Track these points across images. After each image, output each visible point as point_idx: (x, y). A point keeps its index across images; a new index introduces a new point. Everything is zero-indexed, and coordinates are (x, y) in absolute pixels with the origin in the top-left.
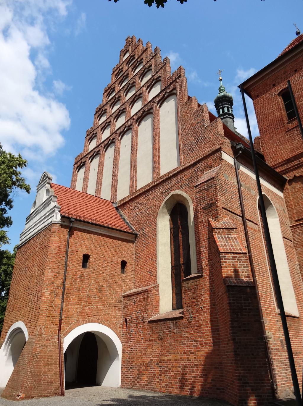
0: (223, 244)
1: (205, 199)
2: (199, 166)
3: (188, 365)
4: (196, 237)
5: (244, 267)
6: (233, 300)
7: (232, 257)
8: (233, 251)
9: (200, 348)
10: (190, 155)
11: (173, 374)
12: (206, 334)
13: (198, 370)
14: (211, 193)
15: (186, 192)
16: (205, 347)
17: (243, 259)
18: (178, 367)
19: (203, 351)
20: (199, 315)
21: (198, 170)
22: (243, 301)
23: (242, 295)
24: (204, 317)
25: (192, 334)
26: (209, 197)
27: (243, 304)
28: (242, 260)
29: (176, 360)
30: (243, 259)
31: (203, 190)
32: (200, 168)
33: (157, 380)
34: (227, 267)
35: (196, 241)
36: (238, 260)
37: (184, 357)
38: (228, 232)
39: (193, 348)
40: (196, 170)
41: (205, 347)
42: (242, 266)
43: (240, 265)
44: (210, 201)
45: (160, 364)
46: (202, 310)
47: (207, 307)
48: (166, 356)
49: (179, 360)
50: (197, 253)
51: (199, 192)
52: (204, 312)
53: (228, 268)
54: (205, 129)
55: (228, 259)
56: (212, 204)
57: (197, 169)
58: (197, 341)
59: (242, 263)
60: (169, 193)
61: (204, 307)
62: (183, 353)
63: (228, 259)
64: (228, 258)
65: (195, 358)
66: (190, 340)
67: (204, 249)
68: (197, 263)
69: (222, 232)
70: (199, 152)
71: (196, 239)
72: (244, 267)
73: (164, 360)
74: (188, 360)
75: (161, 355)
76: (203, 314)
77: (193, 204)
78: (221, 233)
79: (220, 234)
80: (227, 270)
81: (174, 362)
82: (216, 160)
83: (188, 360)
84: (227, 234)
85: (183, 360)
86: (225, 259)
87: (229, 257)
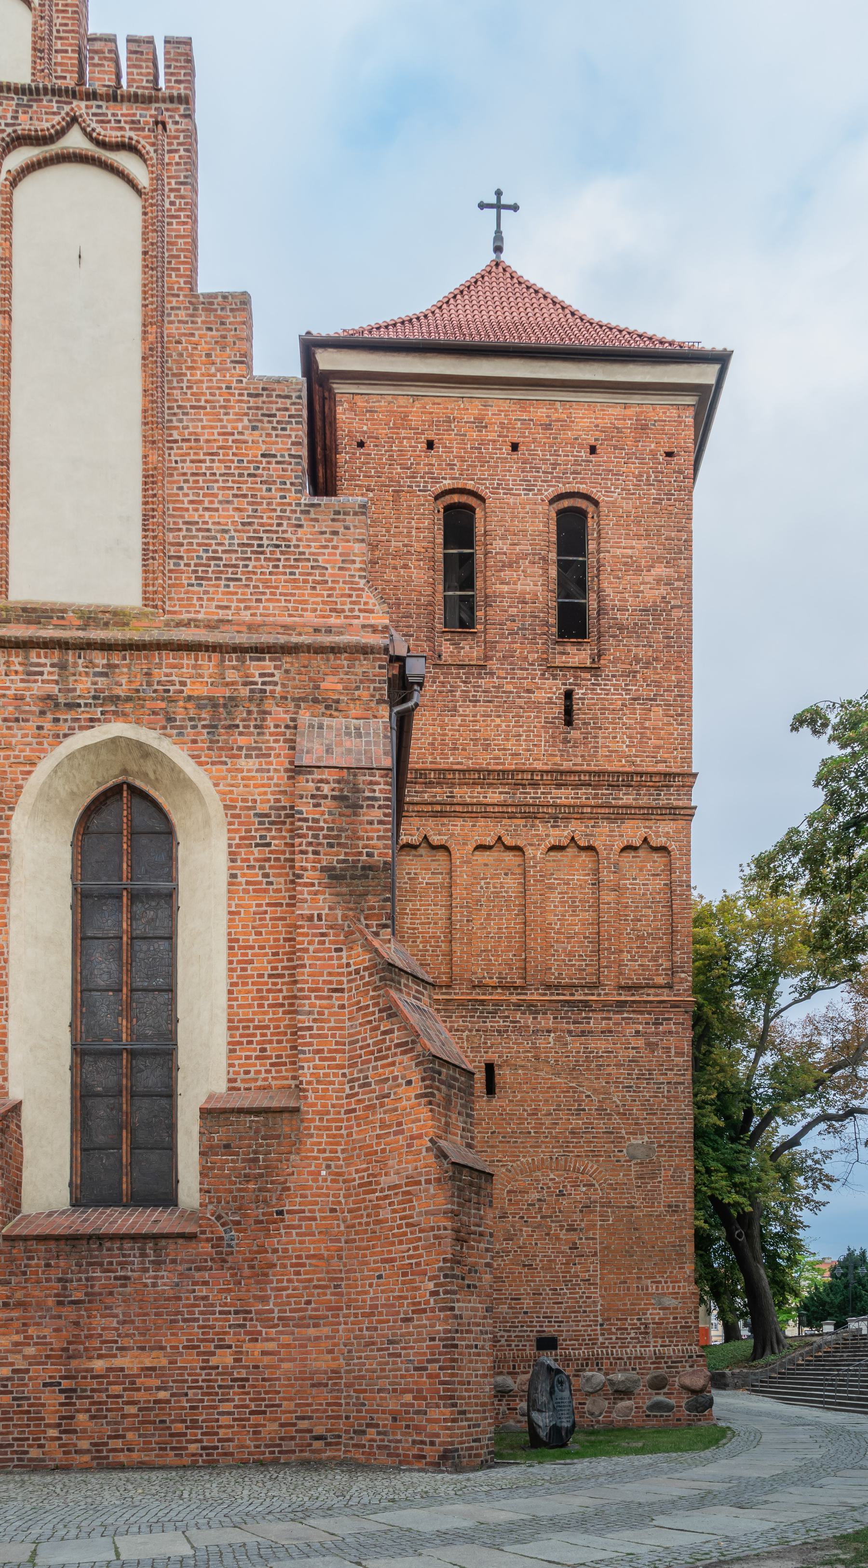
2: (273, 675)
3: (203, 1381)
9: (260, 1333)
10: (211, 590)
11: (132, 1410)
12: (290, 1292)
13: (248, 1393)
16: (280, 1328)
18: (158, 1389)
19: (273, 1340)
20: (268, 1236)
21: (268, 688)
24: (288, 1243)
25: (229, 1290)
29: (153, 1369)
33: (53, 1433)
37: (191, 1360)
39: (232, 1331)
41: (280, 1328)
45: (65, 1383)
46: (283, 1220)
47: (303, 1211)
48: (100, 1357)
49: (161, 1368)
54: (302, 512)
57: (264, 683)
58: (250, 1312)
61: (289, 1212)
62: (184, 1347)
65: (236, 1360)
66: (218, 1309)
70: (259, 601)
73: (92, 1370)
74: (202, 1368)
75: (67, 1354)
76: (283, 1231)
81: (139, 1376)
83: (202, 1368)
85: (180, 1368)
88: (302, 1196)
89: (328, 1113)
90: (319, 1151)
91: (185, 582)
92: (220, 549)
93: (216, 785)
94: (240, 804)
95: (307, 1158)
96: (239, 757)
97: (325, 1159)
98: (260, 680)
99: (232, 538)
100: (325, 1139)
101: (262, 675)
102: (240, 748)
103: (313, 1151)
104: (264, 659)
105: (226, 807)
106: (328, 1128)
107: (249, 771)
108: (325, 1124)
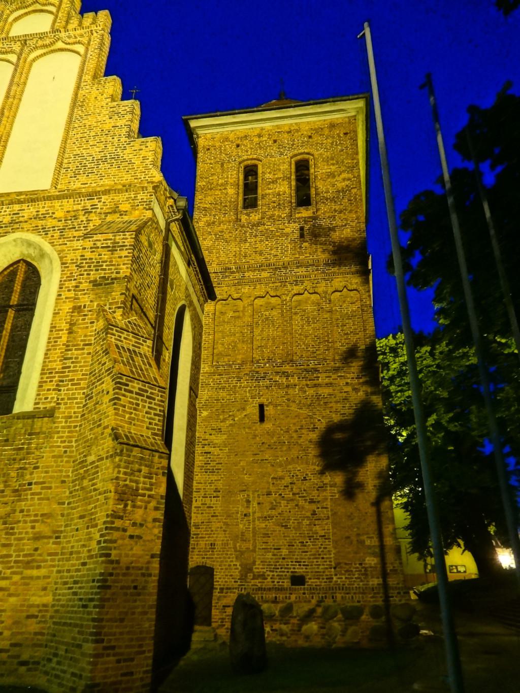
0: (125, 360)
1: (102, 266)
2: (97, 205)
4: (49, 338)
5: (155, 414)
6: (125, 473)
7: (140, 389)
8: (143, 379)
14: (119, 259)
15: (53, 242)
17: (157, 398)
20: (19, 500)
21: (94, 210)
22: (142, 479)
23: (143, 468)
24: (31, 505)
26: (112, 265)
27: (141, 485)
28: (154, 399)
30: (157, 398)
31: (102, 247)
32: (97, 208)
34: (124, 406)
35: (48, 346)
36: (148, 397)
38: (136, 342)
40: (88, 209)
42: (151, 411)
43: (149, 408)
44: (112, 273)
46: (31, 489)
50: (43, 370)
51: (91, 248)
52: (32, 494)
53: (126, 409)
55: (131, 392)
56: (116, 279)
57: (92, 209)
59: (153, 406)
60: (10, 232)
61: (36, 483)
63: (131, 392)
64: (132, 389)
67: (72, 363)
68: (38, 391)
69: (125, 338)
71: (49, 343)
72: (155, 414)
76: (29, 497)
77: (63, 271)
78: (122, 339)
79: (120, 341)
80: (124, 411)
82: (138, 205)
84: (133, 345)
86: (125, 390)
87: (133, 387)
88: (47, 472)
89: (71, 417)
90: (62, 442)
91: (69, 176)
92: (87, 162)
93: (59, 254)
94: (69, 261)
95: (53, 447)
96: (73, 241)
97: (64, 447)
98: (90, 208)
99: (94, 158)
100: (67, 434)
101: (91, 206)
102: (74, 237)
103: (57, 442)
104: (94, 199)
105: (62, 264)
106: (69, 427)
107: (77, 246)
108: (68, 424)
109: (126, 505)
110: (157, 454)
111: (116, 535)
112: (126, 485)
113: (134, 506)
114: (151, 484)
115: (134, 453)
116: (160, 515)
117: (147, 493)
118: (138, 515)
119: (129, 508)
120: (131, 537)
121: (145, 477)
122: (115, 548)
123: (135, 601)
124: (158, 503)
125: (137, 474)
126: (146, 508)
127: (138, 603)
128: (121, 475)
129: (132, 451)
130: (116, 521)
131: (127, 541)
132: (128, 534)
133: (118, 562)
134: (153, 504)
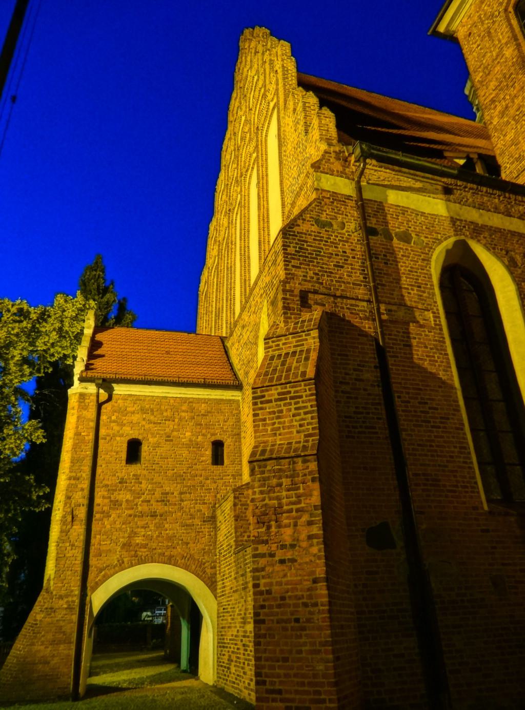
6: (261, 492)
22: (284, 493)
23: (284, 480)
109: (269, 527)
110: (300, 460)
111: (262, 562)
112: (266, 505)
113: (279, 527)
114: (298, 496)
115: (269, 468)
116: (316, 530)
117: (294, 507)
118: (287, 534)
119: (273, 529)
120: (282, 562)
121: (288, 490)
122: (263, 577)
123: (301, 637)
124: (311, 515)
125: (277, 489)
126: (296, 525)
127: (303, 640)
128: (257, 496)
129: (265, 466)
130: (260, 546)
131: (278, 567)
132: (277, 558)
133: (269, 592)
134: (305, 518)
